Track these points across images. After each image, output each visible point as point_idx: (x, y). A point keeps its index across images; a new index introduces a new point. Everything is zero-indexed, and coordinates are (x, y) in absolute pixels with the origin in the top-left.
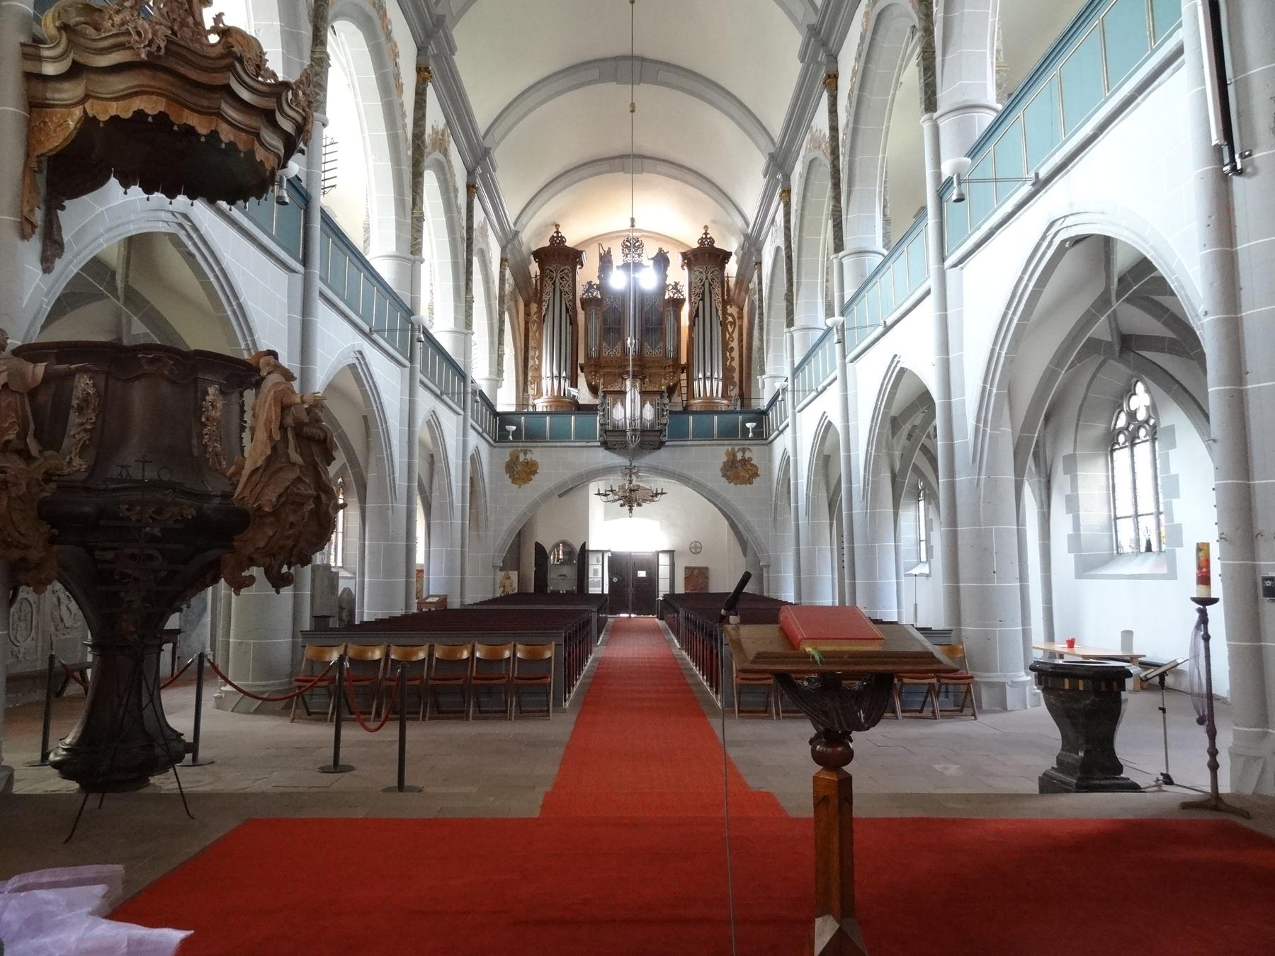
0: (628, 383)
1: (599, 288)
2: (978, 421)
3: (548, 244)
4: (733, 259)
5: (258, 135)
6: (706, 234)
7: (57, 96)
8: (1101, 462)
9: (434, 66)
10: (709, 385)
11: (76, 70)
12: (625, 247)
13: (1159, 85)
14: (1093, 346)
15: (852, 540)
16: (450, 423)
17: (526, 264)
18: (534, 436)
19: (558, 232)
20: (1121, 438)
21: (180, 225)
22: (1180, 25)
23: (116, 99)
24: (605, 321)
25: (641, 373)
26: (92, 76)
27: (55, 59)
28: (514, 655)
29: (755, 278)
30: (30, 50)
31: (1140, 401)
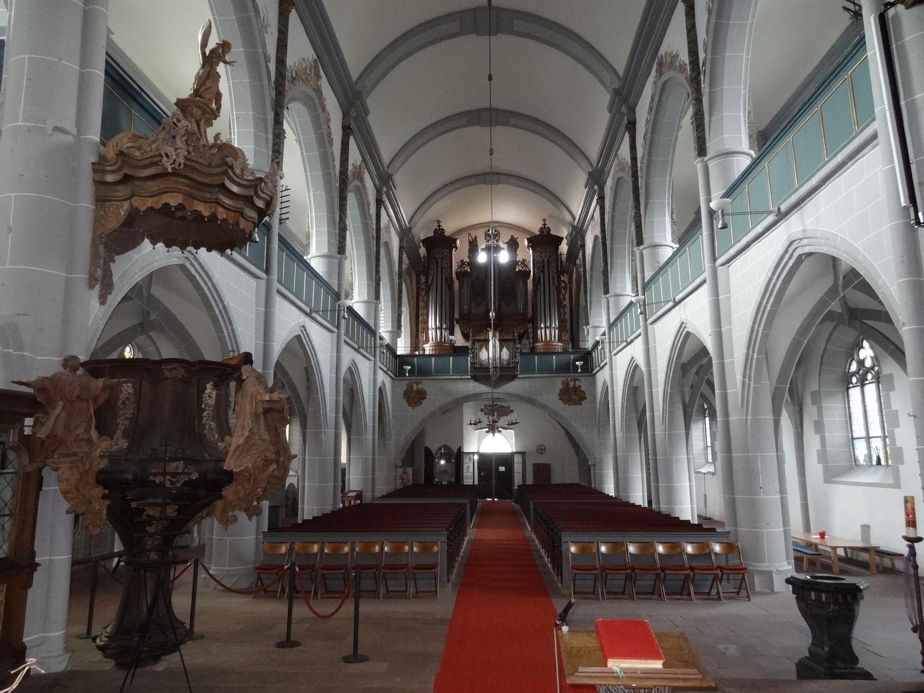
0: (491, 334)
1: (469, 264)
2: (744, 377)
3: (432, 234)
4: (565, 242)
5: (242, 214)
6: (544, 225)
7: (114, 194)
8: (839, 397)
9: (355, 125)
10: (549, 331)
11: (126, 179)
12: (487, 235)
13: (863, 156)
14: (831, 316)
15: (655, 454)
16: (365, 367)
17: (418, 248)
19: (439, 226)
20: (854, 380)
21: (187, 258)
22: (874, 119)
23: (150, 197)
25: (500, 326)
26: (136, 182)
27: (112, 172)
28: (412, 549)
29: (580, 256)
30: (97, 167)
31: (866, 353)
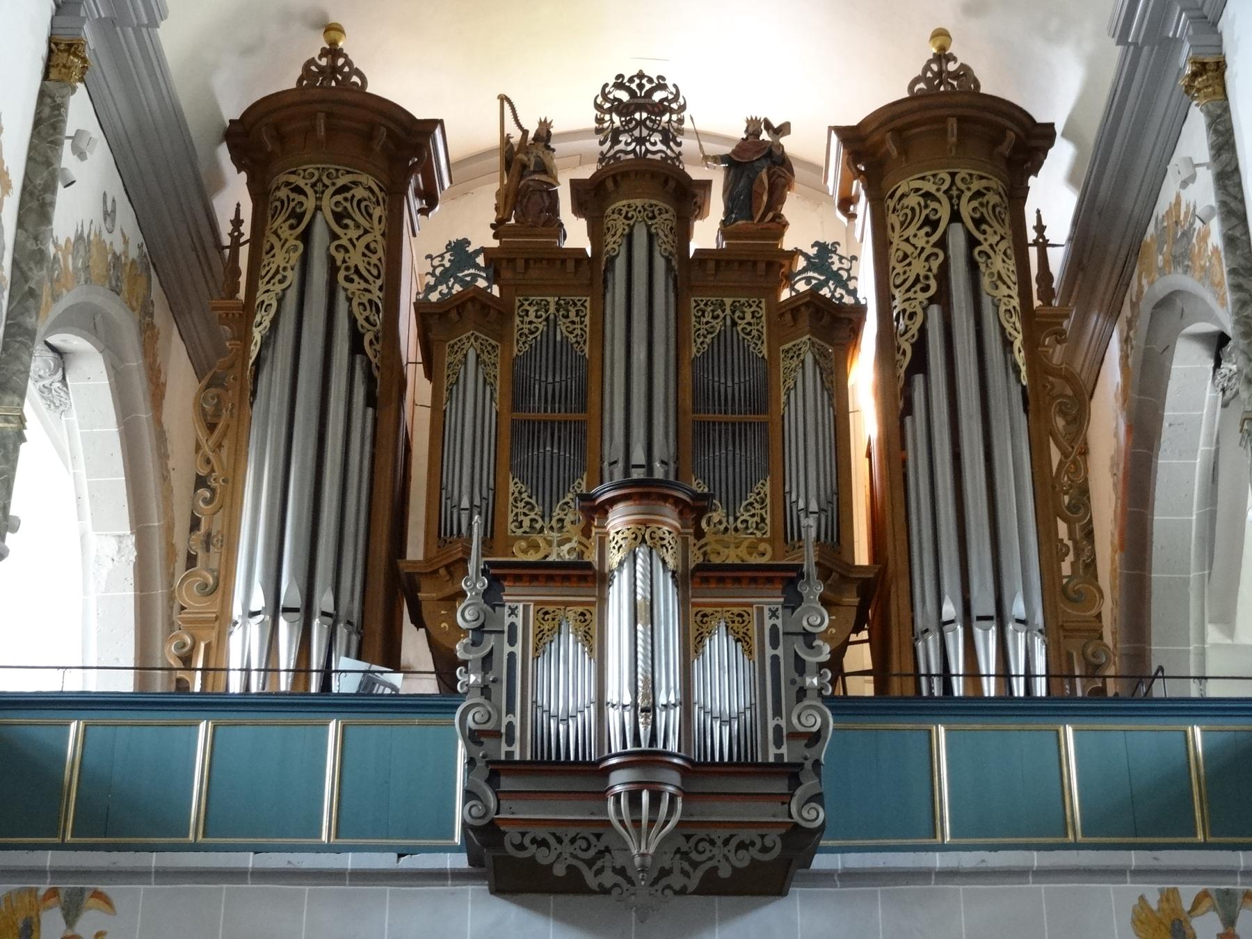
4: (1061, 156)
6: (942, 56)
17: (204, 190)
19: (333, 52)
24: (519, 395)
29: (1195, 139)
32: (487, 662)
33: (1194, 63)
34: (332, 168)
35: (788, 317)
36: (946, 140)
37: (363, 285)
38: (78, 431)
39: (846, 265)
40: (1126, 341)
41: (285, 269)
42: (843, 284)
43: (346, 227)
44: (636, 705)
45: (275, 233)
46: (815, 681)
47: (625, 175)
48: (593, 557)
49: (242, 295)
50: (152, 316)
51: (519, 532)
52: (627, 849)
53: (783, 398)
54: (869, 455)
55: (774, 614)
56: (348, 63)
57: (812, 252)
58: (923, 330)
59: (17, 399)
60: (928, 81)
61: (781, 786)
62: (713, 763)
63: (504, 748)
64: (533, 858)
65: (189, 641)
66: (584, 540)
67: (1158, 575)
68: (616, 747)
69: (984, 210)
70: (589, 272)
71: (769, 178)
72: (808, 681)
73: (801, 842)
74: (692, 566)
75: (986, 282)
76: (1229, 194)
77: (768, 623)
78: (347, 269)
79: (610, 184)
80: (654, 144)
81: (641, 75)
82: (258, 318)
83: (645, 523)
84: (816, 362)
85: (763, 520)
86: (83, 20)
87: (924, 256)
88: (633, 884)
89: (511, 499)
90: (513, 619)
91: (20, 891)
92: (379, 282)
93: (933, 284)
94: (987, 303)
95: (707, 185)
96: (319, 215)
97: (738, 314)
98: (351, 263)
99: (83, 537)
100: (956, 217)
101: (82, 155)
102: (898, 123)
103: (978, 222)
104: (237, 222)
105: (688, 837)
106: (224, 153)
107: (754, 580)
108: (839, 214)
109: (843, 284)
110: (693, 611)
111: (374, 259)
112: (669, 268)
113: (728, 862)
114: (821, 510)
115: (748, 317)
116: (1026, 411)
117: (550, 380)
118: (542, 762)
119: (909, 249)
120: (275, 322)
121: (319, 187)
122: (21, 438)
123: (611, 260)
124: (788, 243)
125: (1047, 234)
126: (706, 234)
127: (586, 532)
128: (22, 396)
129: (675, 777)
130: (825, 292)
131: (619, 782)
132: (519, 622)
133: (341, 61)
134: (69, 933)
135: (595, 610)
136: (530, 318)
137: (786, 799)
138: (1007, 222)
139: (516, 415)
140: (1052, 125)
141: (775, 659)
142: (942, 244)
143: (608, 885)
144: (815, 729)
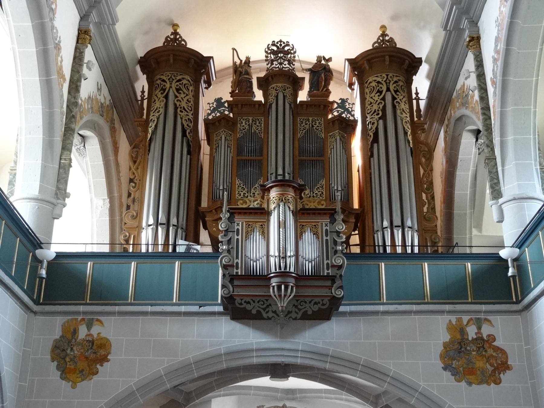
4: (424, 69)
6: (384, 35)
17: (132, 81)
18: (106, 294)
19: (175, 33)
24: (240, 151)
29: (470, 63)
32: (229, 242)
33: (470, 37)
34: (175, 73)
35: (331, 124)
36: (385, 64)
37: (186, 113)
38: (89, 163)
39: (351, 106)
40: (446, 132)
41: (159, 108)
42: (349, 113)
43: (180, 93)
44: (280, 256)
45: (156, 95)
46: (340, 248)
47: (275, 75)
48: (265, 206)
49: (145, 117)
50: (114, 124)
51: (240, 197)
52: (277, 305)
53: (329, 152)
54: (358, 171)
55: (326, 225)
56: (181, 37)
57: (339, 102)
58: (377, 128)
59: (69, 153)
60: (379, 43)
61: (329, 283)
62: (306, 276)
63: (235, 271)
64: (245, 308)
65: (128, 235)
66: (262, 200)
67: (456, 212)
68: (273, 270)
69: (398, 87)
70: (263, 109)
71: (325, 76)
72: (338, 248)
73: (335, 302)
74: (298, 209)
75: (398, 112)
76: (481, 82)
77: (324, 228)
78: (181, 108)
79: (270, 79)
80: (285, 65)
81: (281, 41)
82: (150, 125)
83: (283, 194)
84: (340, 139)
85: (322, 193)
86: (90, 23)
87: (377, 103)
88: (279, 316)
89: (237, 186)
90: (238, 227)
91: (72, 319)
92: (192, 112)
93: (380, 112)
94: (399, 119)
95: (303, 79)
96: (171, 89)
97: (314, 123)
98: (182, 106)
99: (91, 200)
100: (388, 90)
101: (90, 69)
102: (368, 58)
103: (396, 92)
104: (143, 92)
105: (297, 301)
106: (138, 68)
107: (319, 214)
108: (348, 89)
109: (349, 113)
110: (299, 224)
111: (190, 105)
112: (290, 107)
113: (311, 309)
114: (342, 190)
115: (317, 124)
116: (412, 156)
117: (250, 145)
118: (248, 275)
119: (372, 101)
120: (156, 126)
121: (171, 80)
122: (70, 166)
123: (271, 105)
124: (331, 99)
125: (419, 95)
126: (303, 96)
127: (263, 198)
128: (71, 151)
129: (293, 280)
130: (344, 115)
131: (274, 282)
132: (240, 228)
133: (178, 37)
134: (89, 333)
135: (266, 224)
136: (243, 125)
137: (330, 288)
138: (406, 91)
139: (239, 158)
140: (420, 59)
141: (327, 240)
142: (384, 99)
143: (270, 317)
144: (340, 264)
